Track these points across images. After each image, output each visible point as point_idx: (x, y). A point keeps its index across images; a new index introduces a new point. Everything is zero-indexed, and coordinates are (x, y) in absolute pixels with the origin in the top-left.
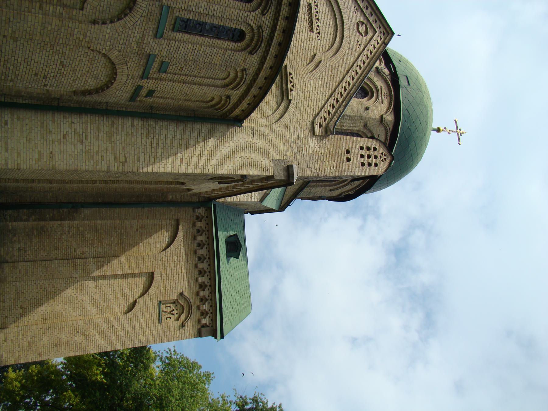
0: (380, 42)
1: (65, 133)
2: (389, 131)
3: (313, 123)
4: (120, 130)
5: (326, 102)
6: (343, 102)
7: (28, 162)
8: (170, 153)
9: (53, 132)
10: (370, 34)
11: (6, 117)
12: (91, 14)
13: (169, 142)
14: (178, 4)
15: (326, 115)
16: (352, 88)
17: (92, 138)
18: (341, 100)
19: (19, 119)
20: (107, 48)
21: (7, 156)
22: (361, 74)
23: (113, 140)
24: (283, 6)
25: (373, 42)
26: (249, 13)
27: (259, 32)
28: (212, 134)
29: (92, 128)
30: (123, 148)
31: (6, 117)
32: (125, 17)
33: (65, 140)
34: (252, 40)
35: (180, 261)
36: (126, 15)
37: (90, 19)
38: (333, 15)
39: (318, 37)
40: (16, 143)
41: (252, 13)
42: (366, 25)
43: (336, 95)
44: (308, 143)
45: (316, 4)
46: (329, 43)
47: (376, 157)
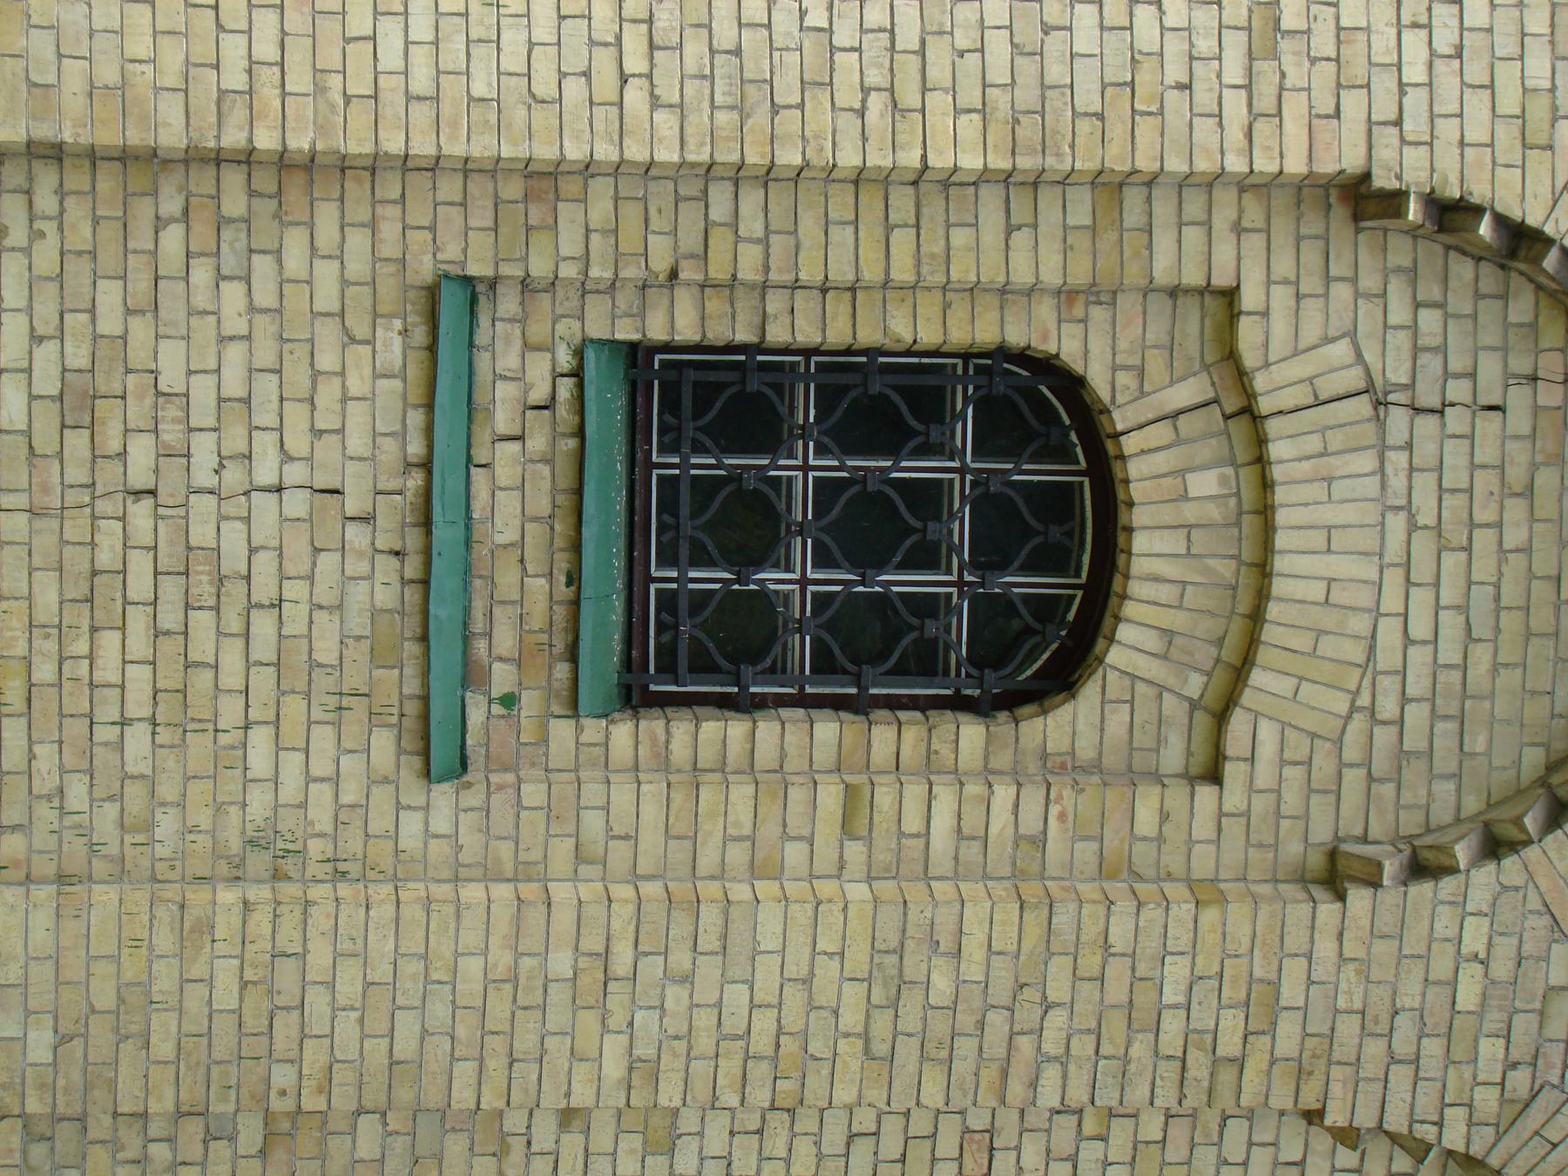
12: (1292, 800)
20: (1486, 1100)
37: (1293, 849)
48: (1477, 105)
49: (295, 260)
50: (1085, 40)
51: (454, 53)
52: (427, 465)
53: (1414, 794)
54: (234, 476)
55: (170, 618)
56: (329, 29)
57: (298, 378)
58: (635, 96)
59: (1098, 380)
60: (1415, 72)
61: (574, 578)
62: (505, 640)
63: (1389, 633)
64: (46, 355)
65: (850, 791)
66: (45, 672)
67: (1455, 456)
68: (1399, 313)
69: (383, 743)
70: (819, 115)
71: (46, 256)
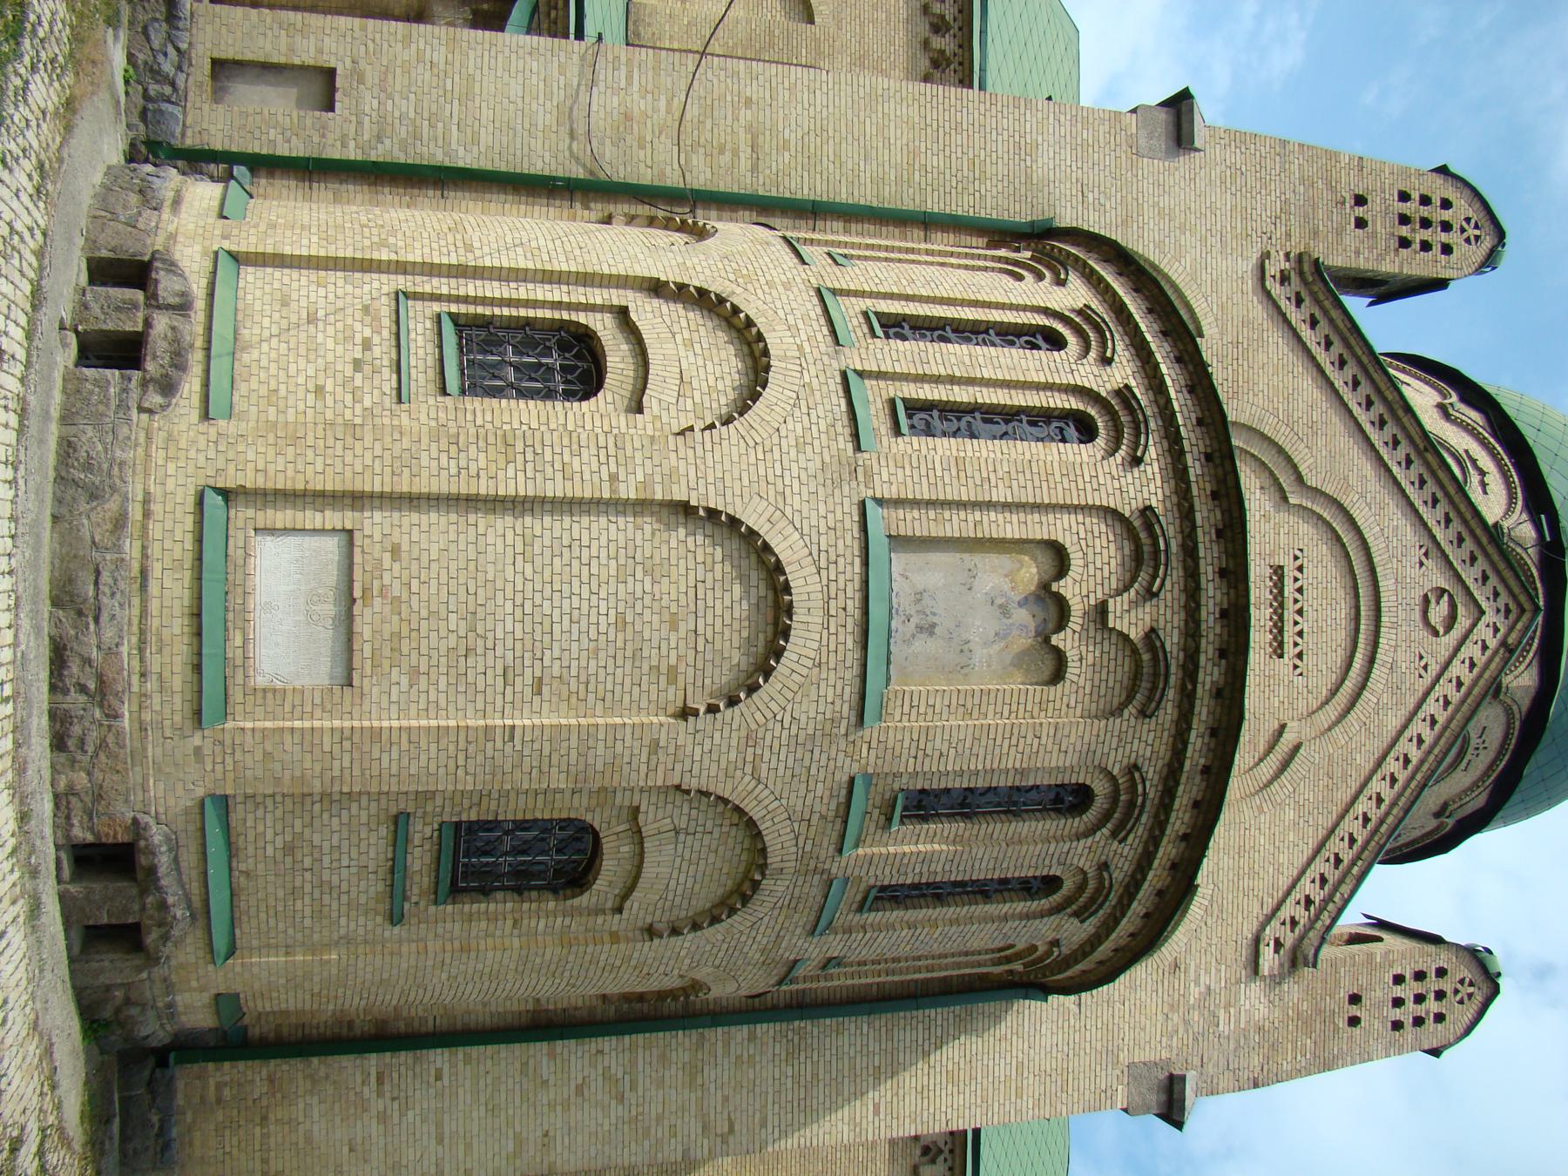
0: (1492, 643)
1: (580, 1081)
2: (1517, 716)
3: (1257, 941)
4: (720, 1052)
5: (1303, 872)
6: (1353, 863)
7: (490, 1164)
9: (551, 1082)
10: (1463, 622)
11: (439, 1059)
15: (1302, 915)
16: (1387, 814)
17: (648, 1085)
18: (1346, 857)
19: (467, 1060)
21: (440, 1155)
22: (1422, 762)
23: (699, 1081)
24: (1173, 815)
25: (1471, 650)
27: (1101, 879)
28: (963, 1027)
29: (648, 1059)
30: (726, 1099)
31: (439, 1059)
33: (580, 1100)
34: (1081, 888)
35: (874, 1160)
36: (732, 911)
37: (640, 924)
38: (1349, 584)
39: (1296, 667)
40: (461, 1121)
41: (1082, 842)
42: (1450, 596)
43: (1337, 846)
44: (1237, 1000)
45: (1298, 563)
46: (1323, 683)
47: (1440, 995)
48: (714, 766)
49: (354, 810)
50: (600, 751)
51: (405, 762)
52: (393, 859)
53: (675, 912)
54: (335, 865)
55: (317, 895)
56: (367, 757)
57: (355, 840)
58: (461, 772)
61: (437, 877)
62: (416, 890)
63: (673, 883)
64: (279, 839)
65: (515, 922)
66: (280, 908)
67: (697, 847)
68: (686, 810)
69: (379, 919)
70: (517, 775)
71: (279, 813)
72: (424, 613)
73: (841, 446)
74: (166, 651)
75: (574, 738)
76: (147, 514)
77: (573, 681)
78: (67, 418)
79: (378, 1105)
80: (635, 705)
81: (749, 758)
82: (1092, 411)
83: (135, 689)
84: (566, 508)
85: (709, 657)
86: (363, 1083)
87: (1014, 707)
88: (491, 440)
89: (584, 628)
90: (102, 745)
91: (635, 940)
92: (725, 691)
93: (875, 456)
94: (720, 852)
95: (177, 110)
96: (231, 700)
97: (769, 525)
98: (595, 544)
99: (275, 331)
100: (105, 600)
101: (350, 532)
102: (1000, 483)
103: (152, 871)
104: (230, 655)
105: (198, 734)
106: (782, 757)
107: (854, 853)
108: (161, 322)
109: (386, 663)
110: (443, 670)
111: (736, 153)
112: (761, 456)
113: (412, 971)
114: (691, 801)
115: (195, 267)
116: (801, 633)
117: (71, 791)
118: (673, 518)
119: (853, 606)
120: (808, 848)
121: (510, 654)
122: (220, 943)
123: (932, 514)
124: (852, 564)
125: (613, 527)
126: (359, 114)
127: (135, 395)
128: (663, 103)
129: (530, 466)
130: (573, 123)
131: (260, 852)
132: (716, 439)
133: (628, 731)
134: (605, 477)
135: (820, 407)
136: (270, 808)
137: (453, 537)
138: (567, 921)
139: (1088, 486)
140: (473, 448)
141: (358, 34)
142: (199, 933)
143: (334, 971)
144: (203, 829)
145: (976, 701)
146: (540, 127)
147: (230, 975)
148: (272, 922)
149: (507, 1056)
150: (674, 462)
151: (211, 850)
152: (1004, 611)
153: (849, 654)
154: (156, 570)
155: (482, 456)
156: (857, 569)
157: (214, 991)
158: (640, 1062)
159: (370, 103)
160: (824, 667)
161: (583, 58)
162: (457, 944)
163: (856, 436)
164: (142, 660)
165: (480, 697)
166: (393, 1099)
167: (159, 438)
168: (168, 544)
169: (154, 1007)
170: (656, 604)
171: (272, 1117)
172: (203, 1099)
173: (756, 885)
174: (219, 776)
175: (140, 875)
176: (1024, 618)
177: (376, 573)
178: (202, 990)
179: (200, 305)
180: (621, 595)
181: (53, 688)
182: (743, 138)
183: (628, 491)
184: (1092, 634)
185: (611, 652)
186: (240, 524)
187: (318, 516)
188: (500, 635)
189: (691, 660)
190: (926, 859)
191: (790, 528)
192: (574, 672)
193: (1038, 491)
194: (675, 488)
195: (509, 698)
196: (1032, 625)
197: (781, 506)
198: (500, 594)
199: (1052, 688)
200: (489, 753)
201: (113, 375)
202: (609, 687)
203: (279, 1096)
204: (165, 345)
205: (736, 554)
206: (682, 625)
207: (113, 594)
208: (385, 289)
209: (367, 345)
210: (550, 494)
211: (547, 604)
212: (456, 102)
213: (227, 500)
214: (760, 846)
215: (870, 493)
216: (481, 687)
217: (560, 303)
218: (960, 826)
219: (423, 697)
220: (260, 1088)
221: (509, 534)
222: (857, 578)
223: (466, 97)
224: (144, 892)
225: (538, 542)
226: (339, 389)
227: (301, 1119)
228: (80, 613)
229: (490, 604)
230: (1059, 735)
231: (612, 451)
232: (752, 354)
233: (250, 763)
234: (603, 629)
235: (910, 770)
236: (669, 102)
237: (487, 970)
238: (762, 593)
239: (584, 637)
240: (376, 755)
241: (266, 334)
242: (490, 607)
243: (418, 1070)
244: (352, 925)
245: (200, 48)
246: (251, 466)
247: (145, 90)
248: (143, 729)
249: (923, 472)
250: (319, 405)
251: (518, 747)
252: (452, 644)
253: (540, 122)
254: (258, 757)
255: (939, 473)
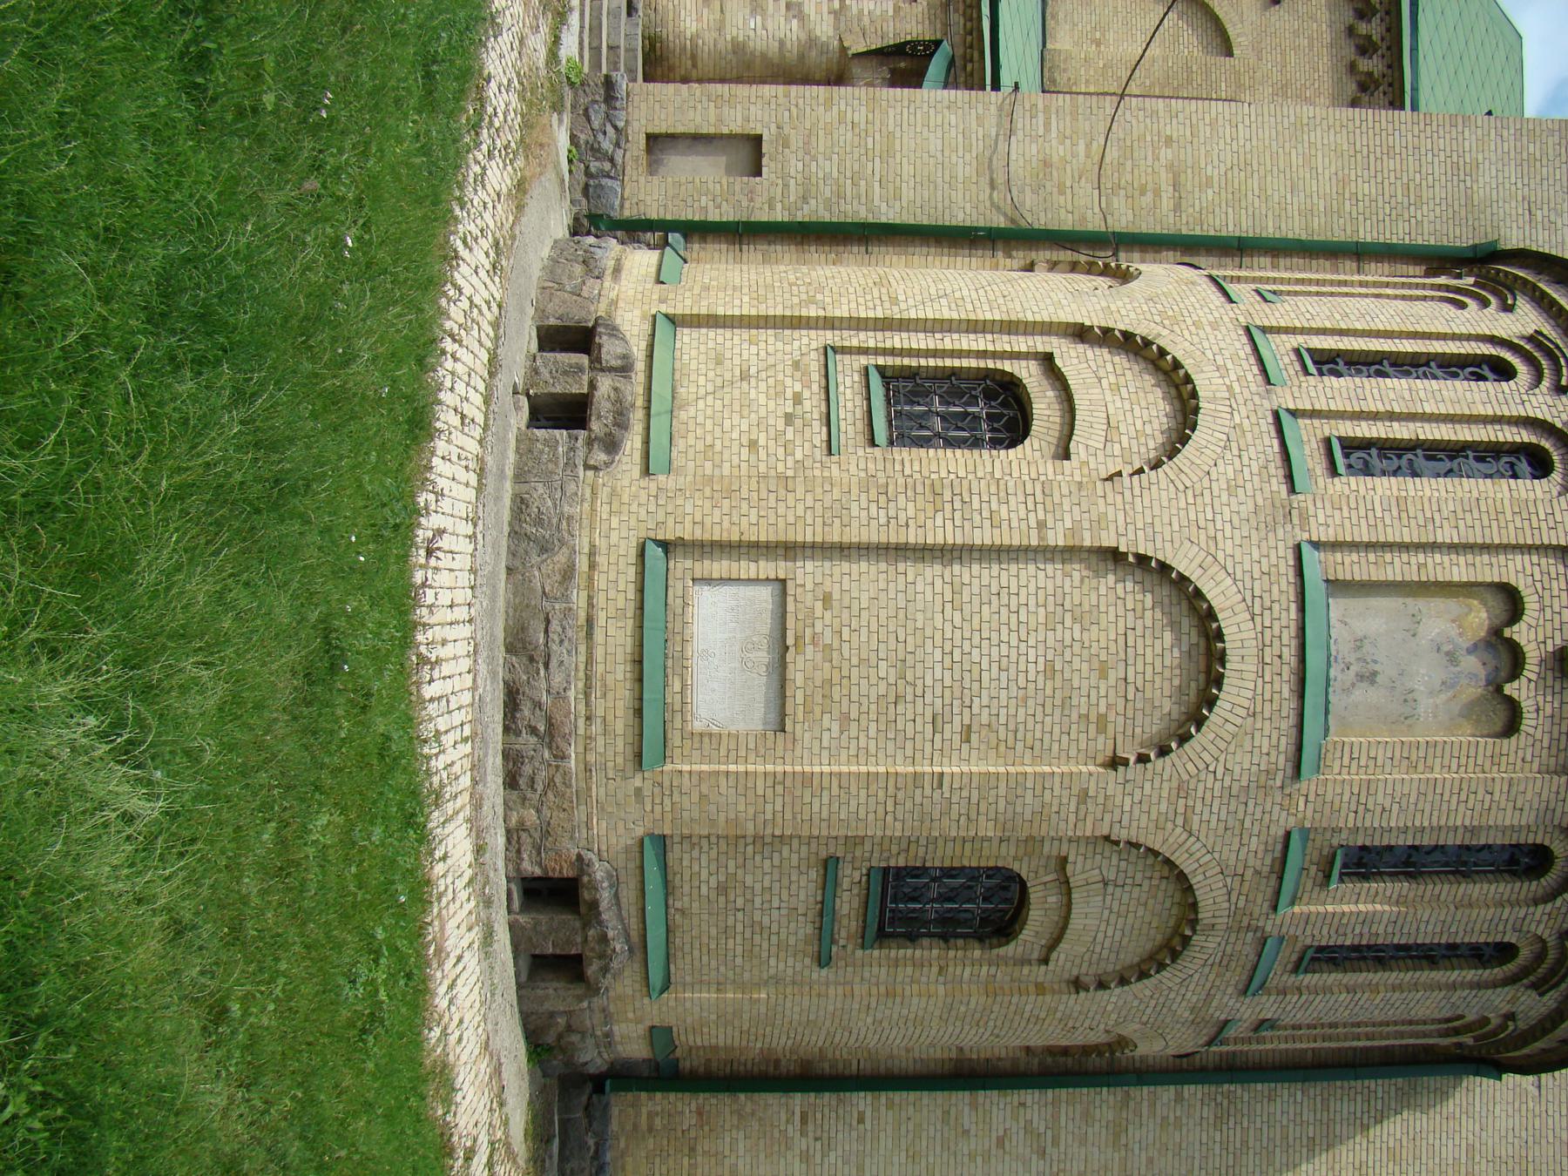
1: (1001, 1133)
4: (1145, 1111)
8: (1278, 1165)
9: (973, 1132)
11: (862, 1102)
13: (1278, 1137)
14: (1309, 928)
19: (890, 1105)
23: (1123, 1141)
26: (1532, 909)
28: (1405, 1101)
30: (1150, 1161)
31: (862, 1102)
32: (1158, 972)
34: (1540, 957)
36: (1161, 967)
37: (1066, 976)
41: (1540, 908)
48: (1144, 817)
49: (786, 852)
50: (1029, 799)
52: (822, 903)
53: (1103, 965)
54: (766, 906)
55: (748, 935)
56: (798, 801)
57: (785, 882)
58: (889, 818)
59: (1024, 876)
60: (1127, 808)
61: (864, 921)
62: (843, 934)
63: (1100, 936)
64: (713, 880)
65: (941, 968)
66: (713, 946)
67: (1125, 899)
68: (1115, 861)
69: (807, 961)
70: (946, 822)
71: (714, 853)
72: (855, 661)
73: (1275, 488)
74: (610, 695)
75: (1002, 785)
76: (592, 566)
77: (1002, 729)
78: (520, 477)
79: (801, 1144)
80: (1063, 754)
81: (1181, 810)
82: (1546, 444)
83: (581, 731)
84: (994, 555)
85: (1139, 705)
86: (788, 1122)
87: (1463, 761)
88: (920, 489)
89: (1013, 676)
90: (550, 784)
91: (1061, 992)
92: (1156, 740)
93: (1310, 498)
94: (1150, 906)
95: (616, 185)
96: (669, 744)
97: (1200, 571)
98: (1023, 591)
99: (710, 388)
100: (554, 647)
101: (784, 581)
102: (1445, 523)
103: (594, 905)
104: (669, 700)
105: (639, 776)
106: (1215, 810)
107: (1289, 910)
108: (605, 384)
109: (818, 710)
110: (873, 716)
111: (1157, 193)
112: (1191, 500)
113: (838, 1013)
114: (1120, 852)
115: (635, 331)
116: (1235, 682)
117: (522, 827)
118: (1102, 565)
119: (1289, 654)
120: (1241, 904)
121: (938, 702)
122: (656, 977)
123: (1372, 557)
124: (1288, 610)
125: (1041, 574)
126: (785, 177)
127: (581, 453)
128: (1081, 148)
129: (958, 515)
130: (993, 174)
131: (695, 891)
132: (1145, 484)
133: (1057, 779)
134: (1033, 524)
135: (1252, 449)
136: (705, 848)
137: (882, 585)
138: (993, 970)
139: (1543, 524)
140: (902, 498)
141: (781, 100)
142: (637, 966)
143: (763, 1010)
144: (642, 867)
145: (1422, 754)
146: (961, 180)
147: (664, 1009)
148: (705, 958)
149: (930, 1103)
150: (1102, 509)
151: (649, 887)
152: (1452, 658)
153: (1285, 704)
154: (601, 619)
155: (911, 505)
156: (1293, 615)
157: (648, 1023)
158: (1063, 1119)
159: (795, 166)
160: (1259, 717)
161: (1000, 109)
162: (882, 989)
163: (1290, 478)
164: (587, 704)
165: (909, 744)
166: (816, 1139)
167: (604, 494)
168: (612, 594)
169: (593, 1035)
170: (1085, 652)
171: (699, 1148)
172: (636, 1127)
173: (1186, 941)
174: (658, 816)
175: (583, 909)
176: (1474, 667)
177: (808, 622)
178: (638, 1021)
179: (640, 366)
180: (1050, 643)
181: (506, 729)
182: (1165, 178)
183: (1056, 538)
184: (1550, 682)
185: (1040, 701)
186: (679, 575)
187: (753, 565)
188: (929, 682)
189: (1120, 709)
190: (1368, 919)
191: (1223, 574)
192: (1002, 720)
193: (1487, 531)
194: (1104, 534)
195: (938, 745)
196: (1482, 673)
197: (1212, 551)
198: (929, 642)
199: (1506, 741)
200: (918, 800)
201: (561, 435)
202: (1038, 735)
203: (706, 1128)
204: (609, 405)
205: (1166, 600)
206: (1112, 675)
207: (561, 642)
208: (814, 345)
209: (798, 399)
210: (978, 542)
211: (976, 652)
212: (877, 160)
213: (666, 553)
214: (1191, 900)
215: (1306, 536)
216: (910, 734)
217: (985, 352)
218: (1403, 887)
219: (854, 743)
220: (689, 1119)
221: (938, 582)
222: (1293, 625)
223: (888, 153)
224: (586, 925)
225: (966, 590)
226: (772, 443)
227: (727, 1153)
228: (532, 659)
229: (919, 652)
230: (1513, 792)
231: (1039, 498)
232: (1180, 396)
233: (686, 805)
234: (1031, 677)
235: (1350, 825)
236: (1088, 146)
237: (912, 1016)
238: (1194, 640)
239: (1013, 685)
240: (807, 799)
241: (702, 392)
242: (919, 654)
243: (841, 1112)
244: (781, 966)
245: (636, 124)
246: (688, 519)
247: (587, 167)
248: (588, 770)
249: (1362, 513)
250: (753, 458)
251: (947, 795)
252: (882, 691)
253: (960, 175)
254: (695, 798)
255: (1379, 514)
